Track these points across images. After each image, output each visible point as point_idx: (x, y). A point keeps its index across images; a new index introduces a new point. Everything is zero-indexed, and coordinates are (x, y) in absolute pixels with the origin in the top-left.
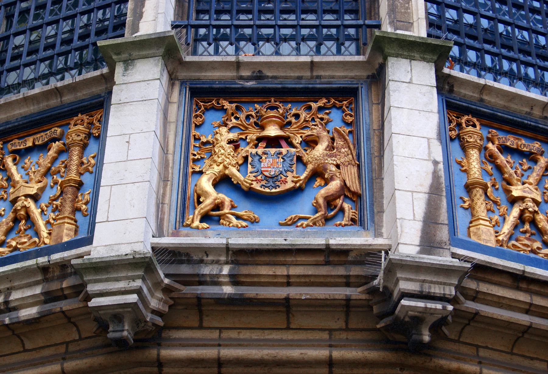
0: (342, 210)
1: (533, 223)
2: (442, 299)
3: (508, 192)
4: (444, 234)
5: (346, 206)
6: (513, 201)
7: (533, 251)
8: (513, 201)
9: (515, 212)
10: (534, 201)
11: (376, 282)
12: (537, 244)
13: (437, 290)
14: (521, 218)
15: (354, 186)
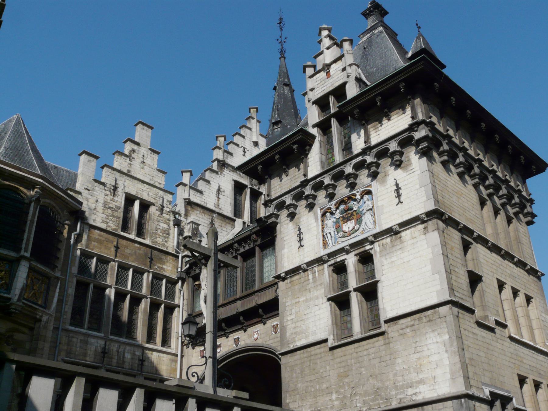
0: (4, 287)
1: (35, 294)
2: (18, 310)
3: (33, 287)
4: (22, 298)
5: (5, 286)
6: (33, 289)
7: (34, 300)
8: (33, 289)
9: (33, 292)
10: (37, 290)
11: (8, 304)
12: (35, 299)
13: (18, 309)
14: (34, 293)
15: (7, 282)
